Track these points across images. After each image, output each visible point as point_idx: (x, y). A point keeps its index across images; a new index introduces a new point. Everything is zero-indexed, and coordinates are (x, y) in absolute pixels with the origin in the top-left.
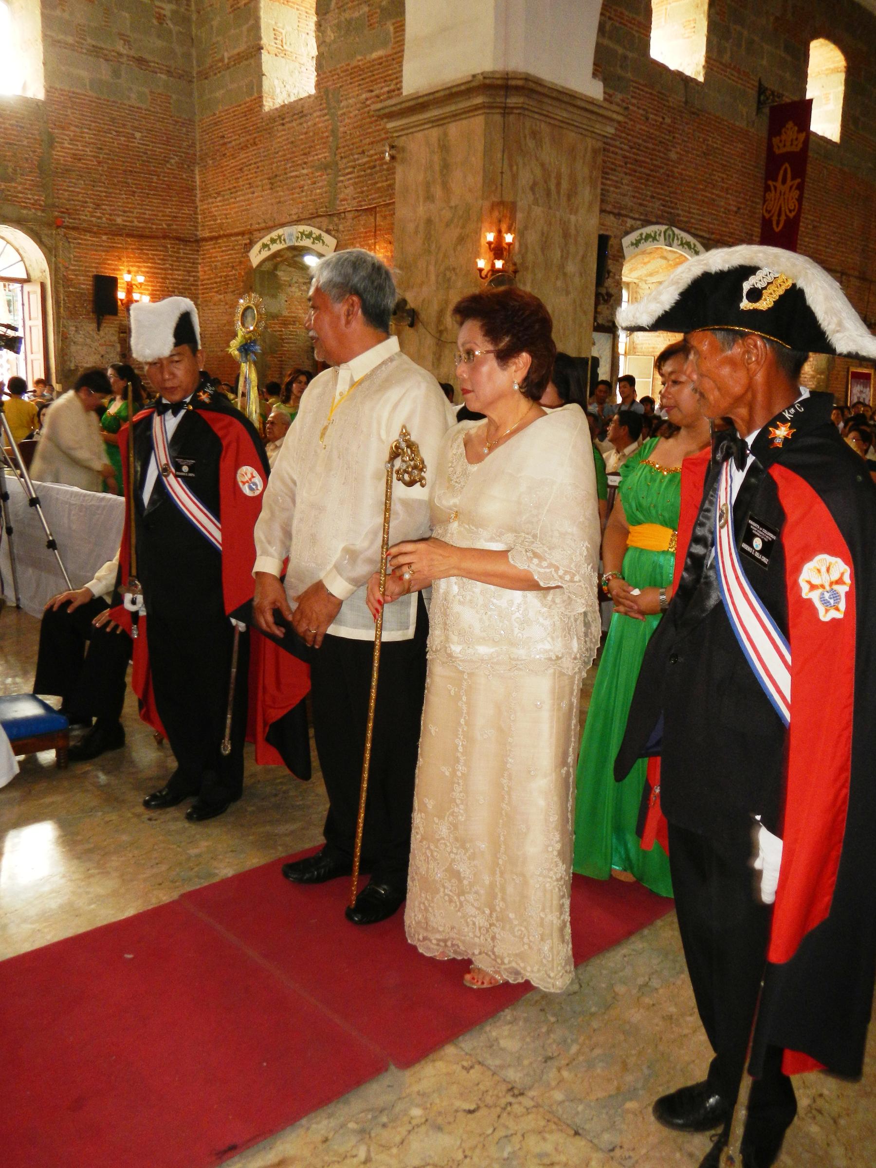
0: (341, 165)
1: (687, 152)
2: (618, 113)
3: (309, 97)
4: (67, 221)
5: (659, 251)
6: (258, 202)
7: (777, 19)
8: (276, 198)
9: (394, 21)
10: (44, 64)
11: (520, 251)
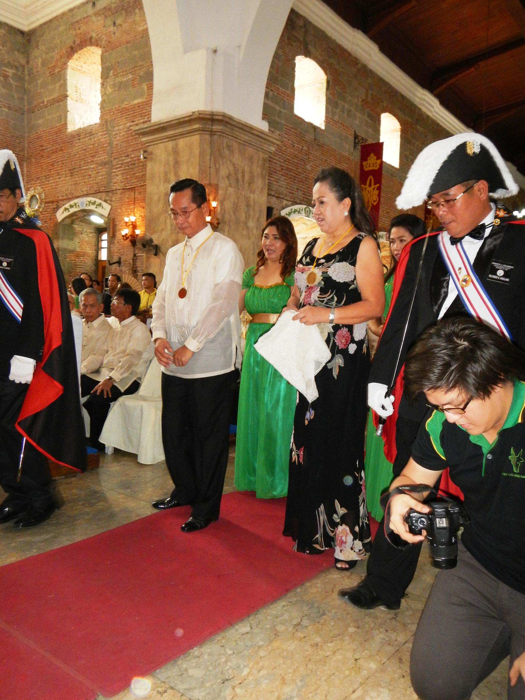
0: (114, 163)
1: (317, 166)
2: (277, 140)
3: (96, 124)
5: (302, 220)
6: (64, 184)
7: (363, 100)
8: (74, 181)
9: (147, 83)
11: (221, 212)
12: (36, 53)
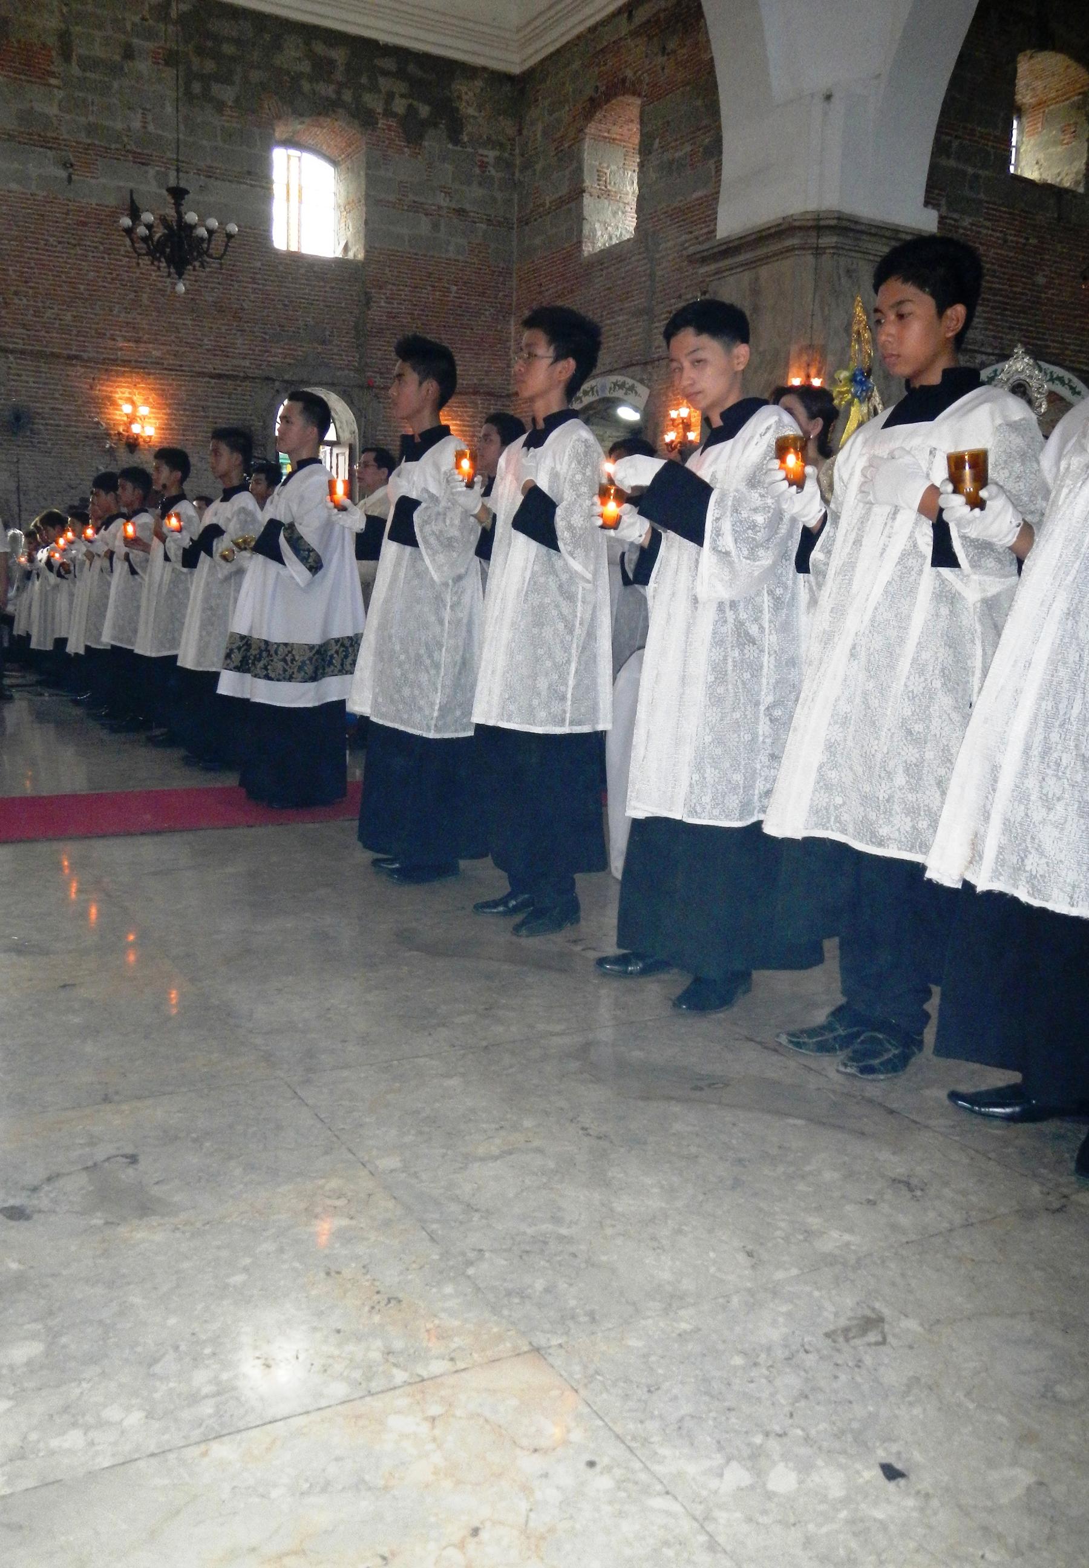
10: (366, 223)
12: (534, 113)
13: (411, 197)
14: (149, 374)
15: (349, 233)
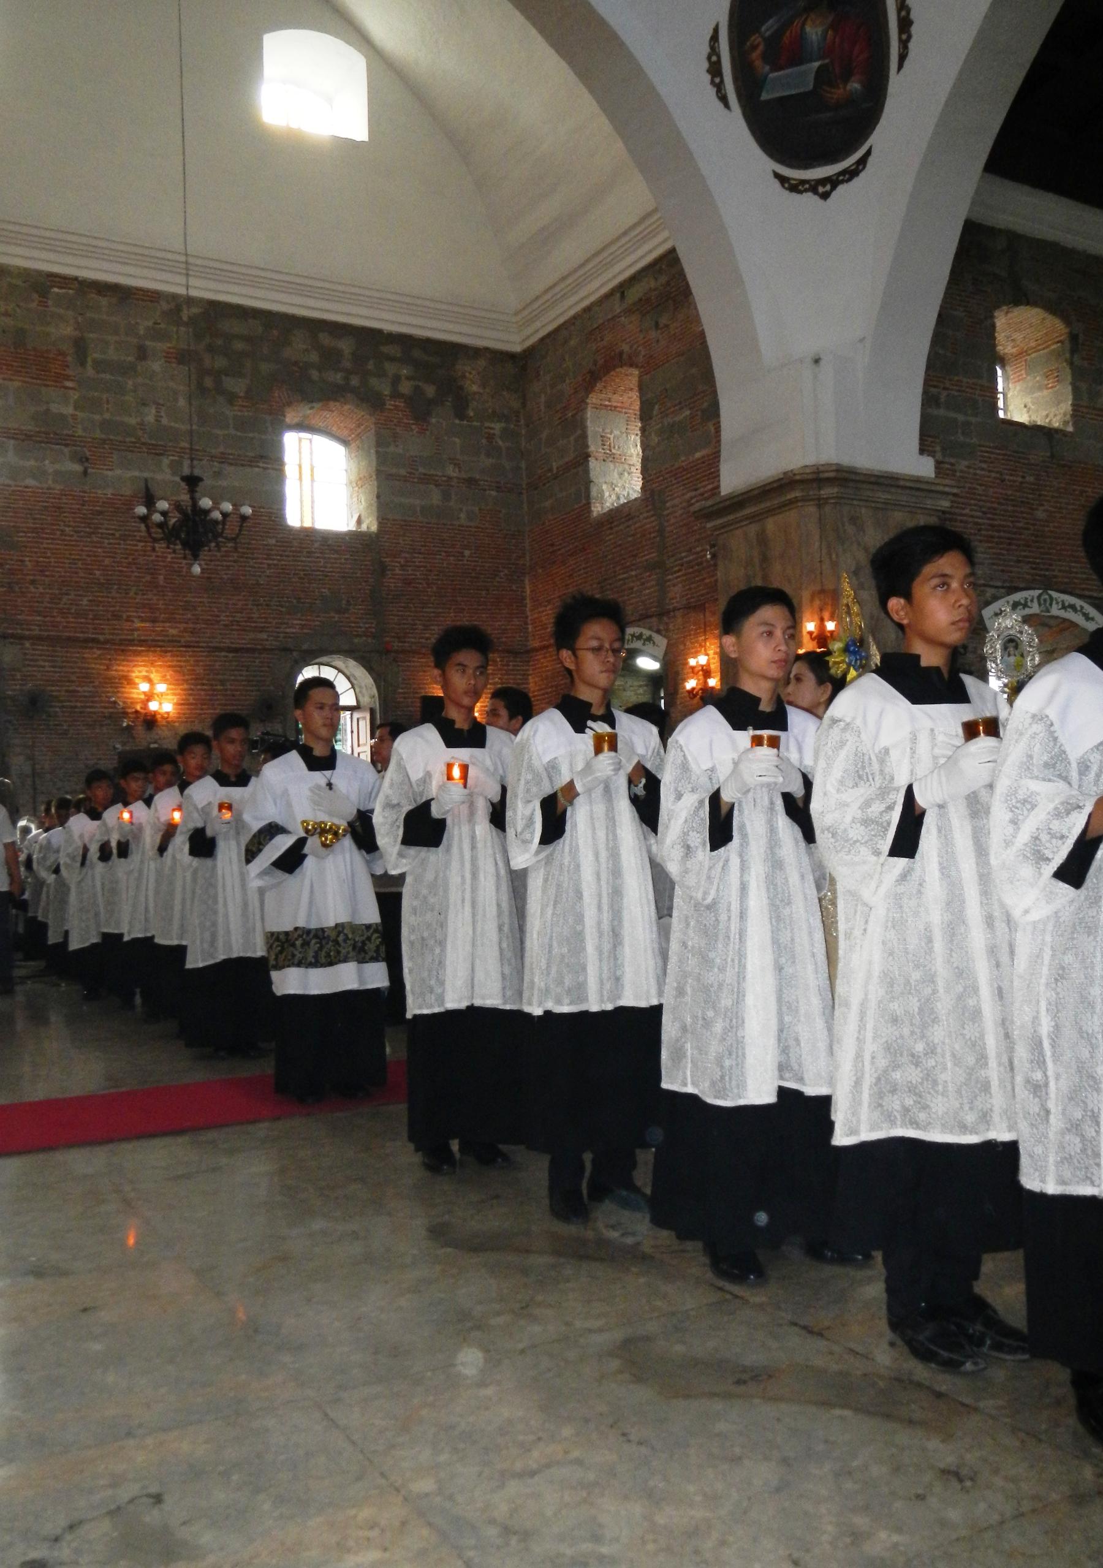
1: (1061, 508)
4: (396, 645)
10: (378, 497)
13: (421, 470)
14: (166, 652)
15: (361, 507)
